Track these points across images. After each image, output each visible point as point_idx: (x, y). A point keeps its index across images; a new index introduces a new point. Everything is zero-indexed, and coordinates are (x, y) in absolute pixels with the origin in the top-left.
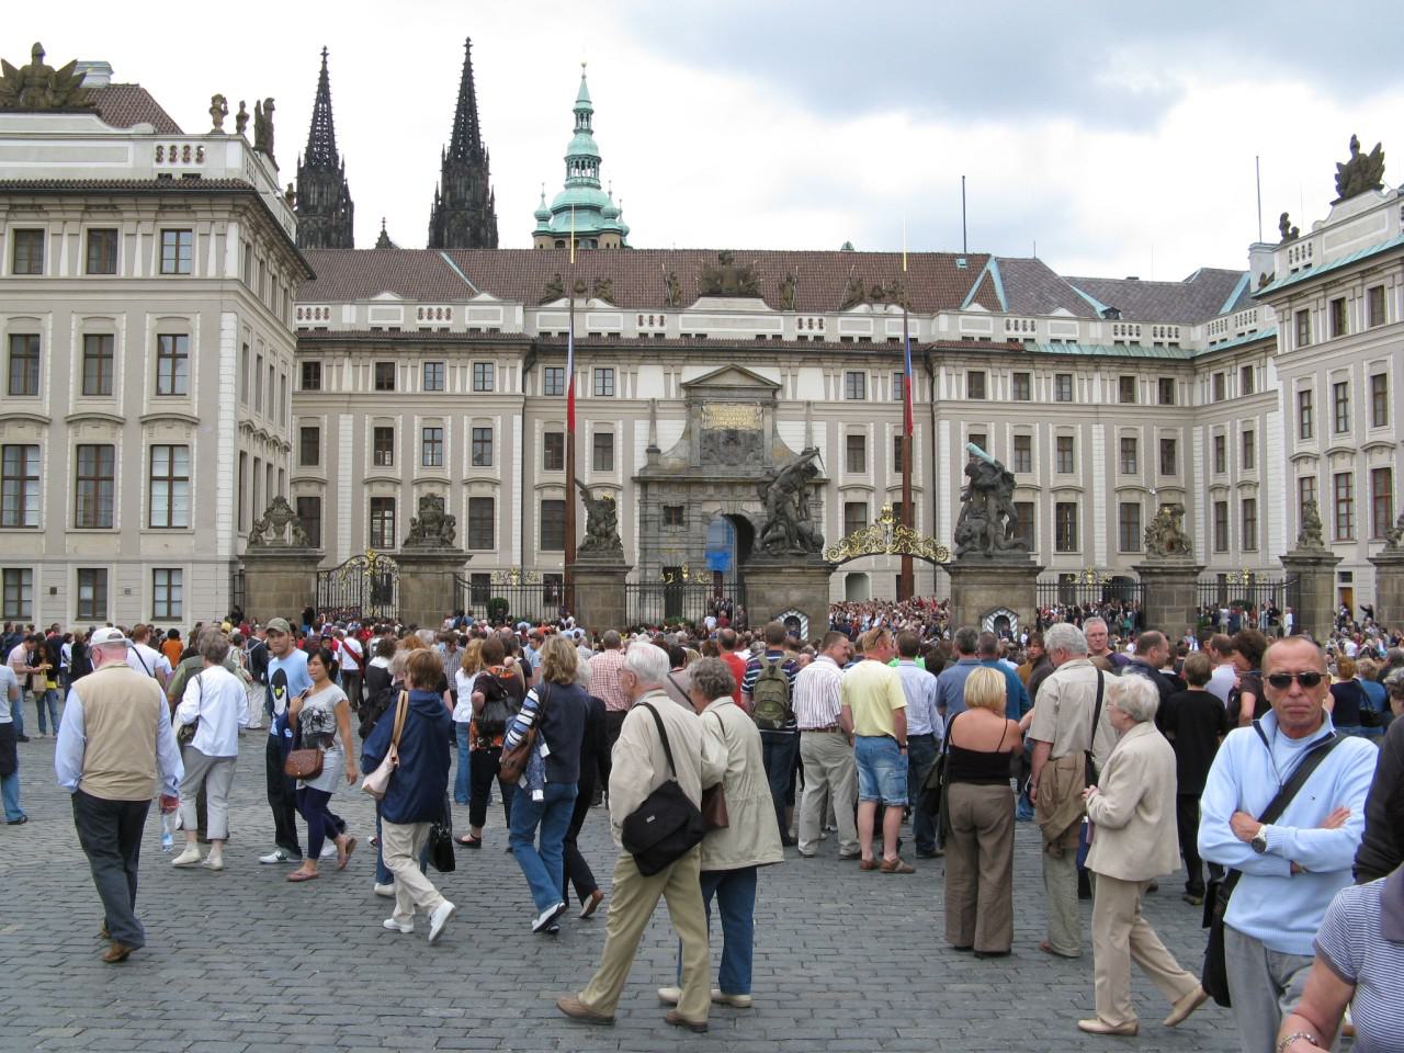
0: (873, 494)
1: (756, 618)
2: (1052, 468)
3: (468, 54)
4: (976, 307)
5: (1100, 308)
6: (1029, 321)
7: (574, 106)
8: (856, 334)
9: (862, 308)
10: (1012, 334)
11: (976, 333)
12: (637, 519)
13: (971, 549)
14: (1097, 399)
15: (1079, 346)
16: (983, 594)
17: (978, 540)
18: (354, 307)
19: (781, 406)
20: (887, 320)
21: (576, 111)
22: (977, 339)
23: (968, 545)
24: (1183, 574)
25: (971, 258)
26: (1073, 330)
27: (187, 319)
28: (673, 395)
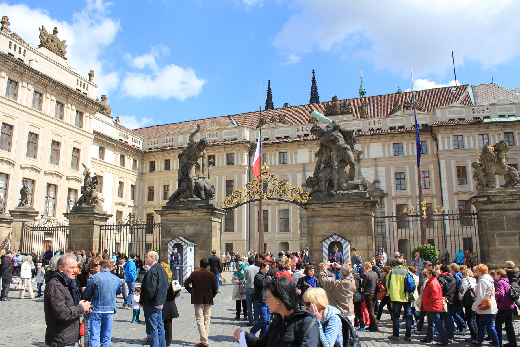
0: (410, 200)
3: (314, 75)
7: (359, 91)
8: (397, 125)
9: (399, 113)
10: (476, 115)
11: (456, 116)
12: (298, 217)
13: (317, 191)
16: (327, 226)
18: (182, 136)
19: (362, 161)
21: (359, 93)
22: (457, 119)
23: (316, 188)
24: (510, 202)
27: (14, 119)
28: (313, 160)
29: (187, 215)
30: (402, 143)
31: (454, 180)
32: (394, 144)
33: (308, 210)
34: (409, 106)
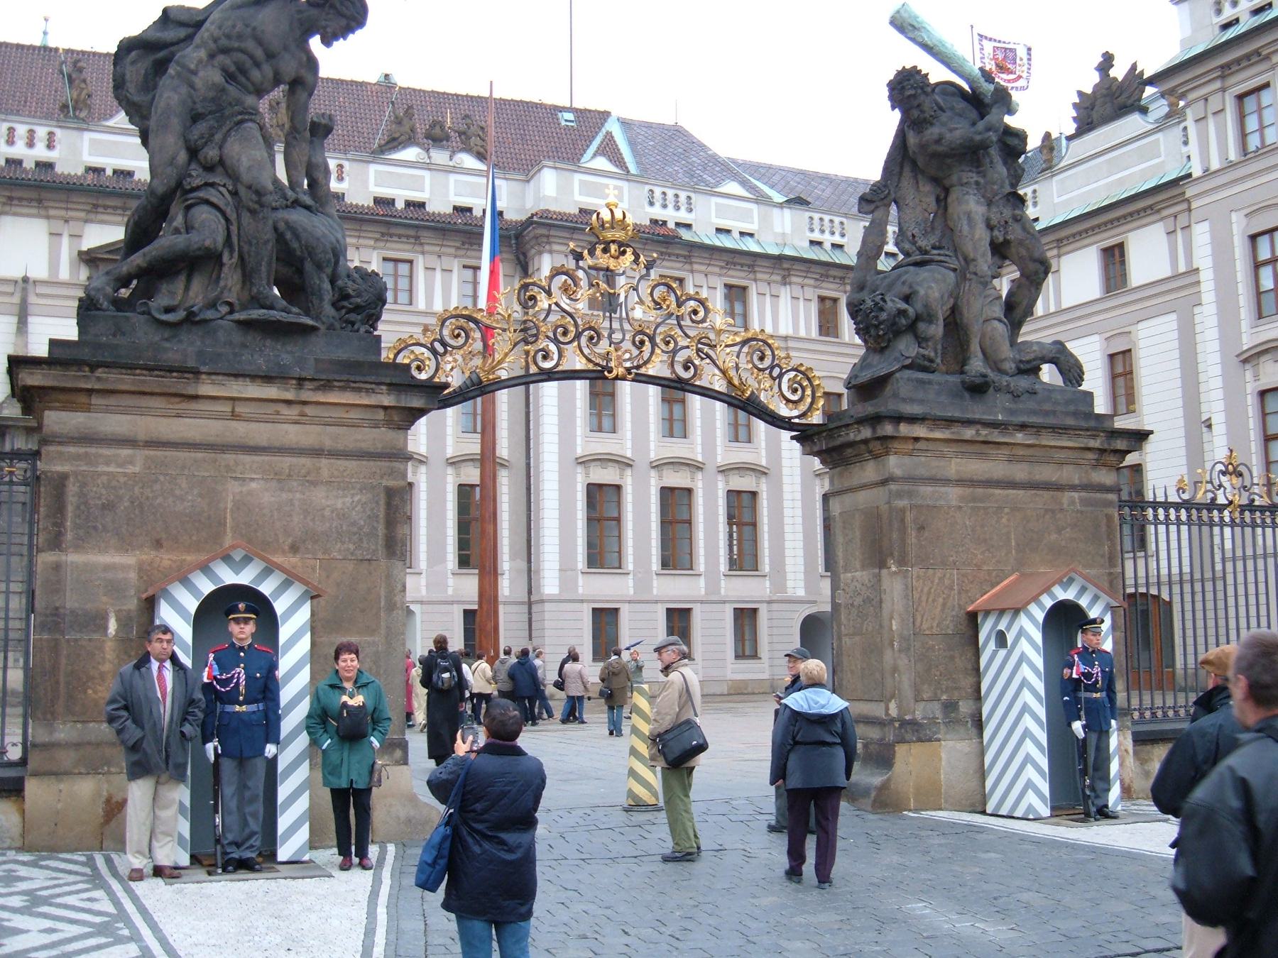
1: (71, 601)
2: (719, 433)
4: (602, 163)
5: (779, 198)
6: (683, 196)
8: (401, 195)
9: (411, 153)
10: (657, 212)
14: (785, 329)
15: (758, 242)
17: (937, 330)
20: (453, 178)
23: (907, 347)
25: (581, 114)
26: (747, 216)
28: (64, 274)
29: (240, 409)
30: (411, 262)
31: (579, 413)
32: (385, 259)
33: (896, 445)
34: (448, 138)
